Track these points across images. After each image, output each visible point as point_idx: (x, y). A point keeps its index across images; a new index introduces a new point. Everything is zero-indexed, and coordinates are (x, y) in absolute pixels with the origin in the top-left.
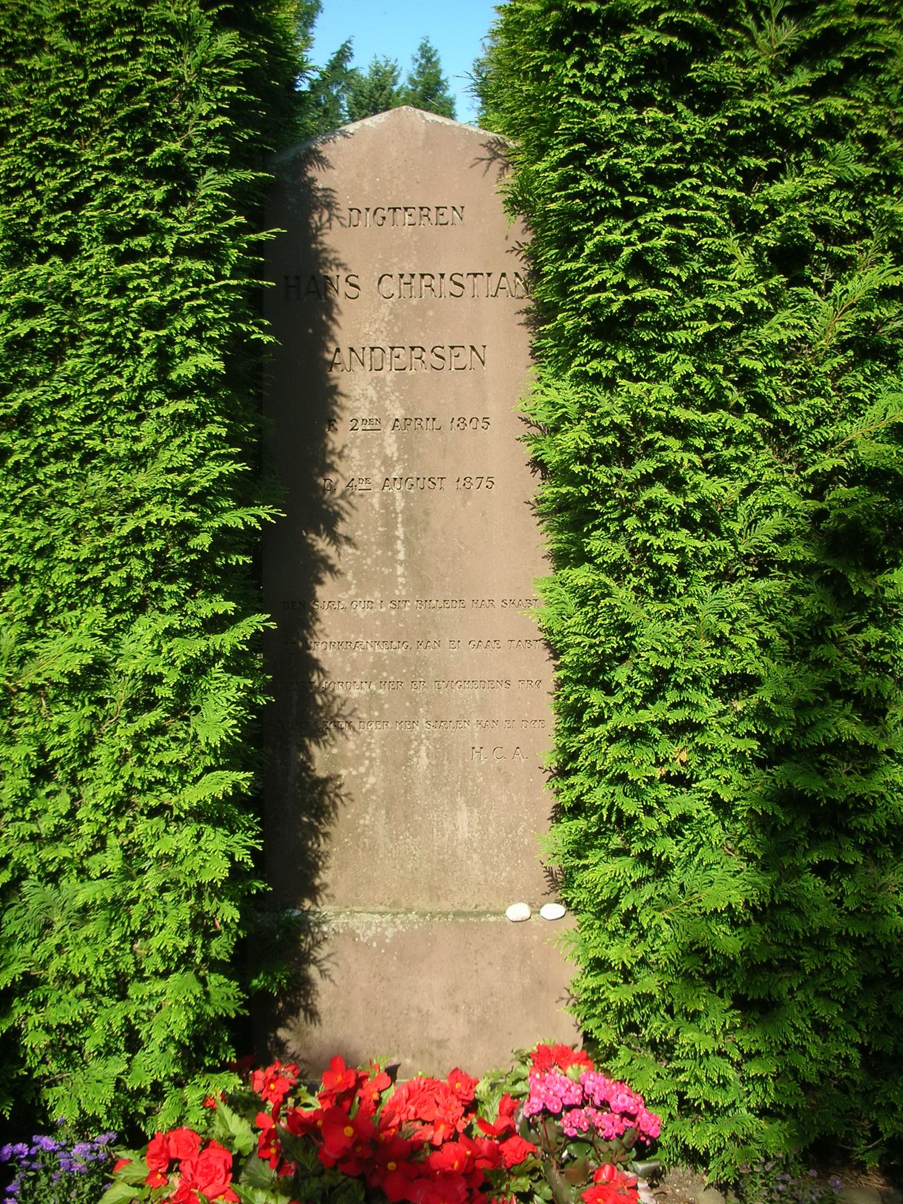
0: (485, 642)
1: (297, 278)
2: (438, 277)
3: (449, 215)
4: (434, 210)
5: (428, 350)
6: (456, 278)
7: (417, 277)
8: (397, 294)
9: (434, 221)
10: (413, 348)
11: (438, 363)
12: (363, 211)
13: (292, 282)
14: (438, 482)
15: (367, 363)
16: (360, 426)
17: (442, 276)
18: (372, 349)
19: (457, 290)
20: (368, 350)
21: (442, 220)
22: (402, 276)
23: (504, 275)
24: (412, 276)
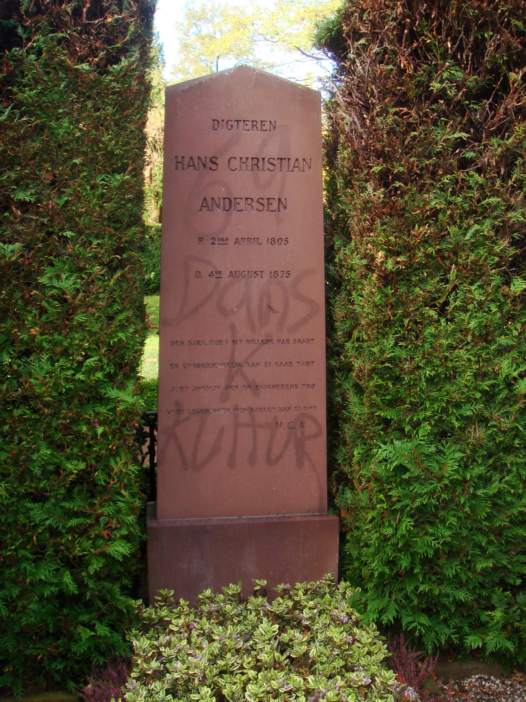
0: (284, 363)
1: (183, 157)
2: (261, 160)
3: (267, 126)
4: (259, 123)
5: (255, 200)
6: (271, 161)
7: (250, 160)
8: (238, 168)
9: (259, 128)
10: (247, 199)
11: (260, 207)
12: (221, 121)
13: (180, 159)
14: (259, 274)
15: (222, 205)
16: (217, 242)
17: (263, 159)
18: (224, 199)
19: (271, 167)
20: (222, 200)
21: (264, 128)
22: (241, 158)
23: (297, 160)
24: (247, 158)
